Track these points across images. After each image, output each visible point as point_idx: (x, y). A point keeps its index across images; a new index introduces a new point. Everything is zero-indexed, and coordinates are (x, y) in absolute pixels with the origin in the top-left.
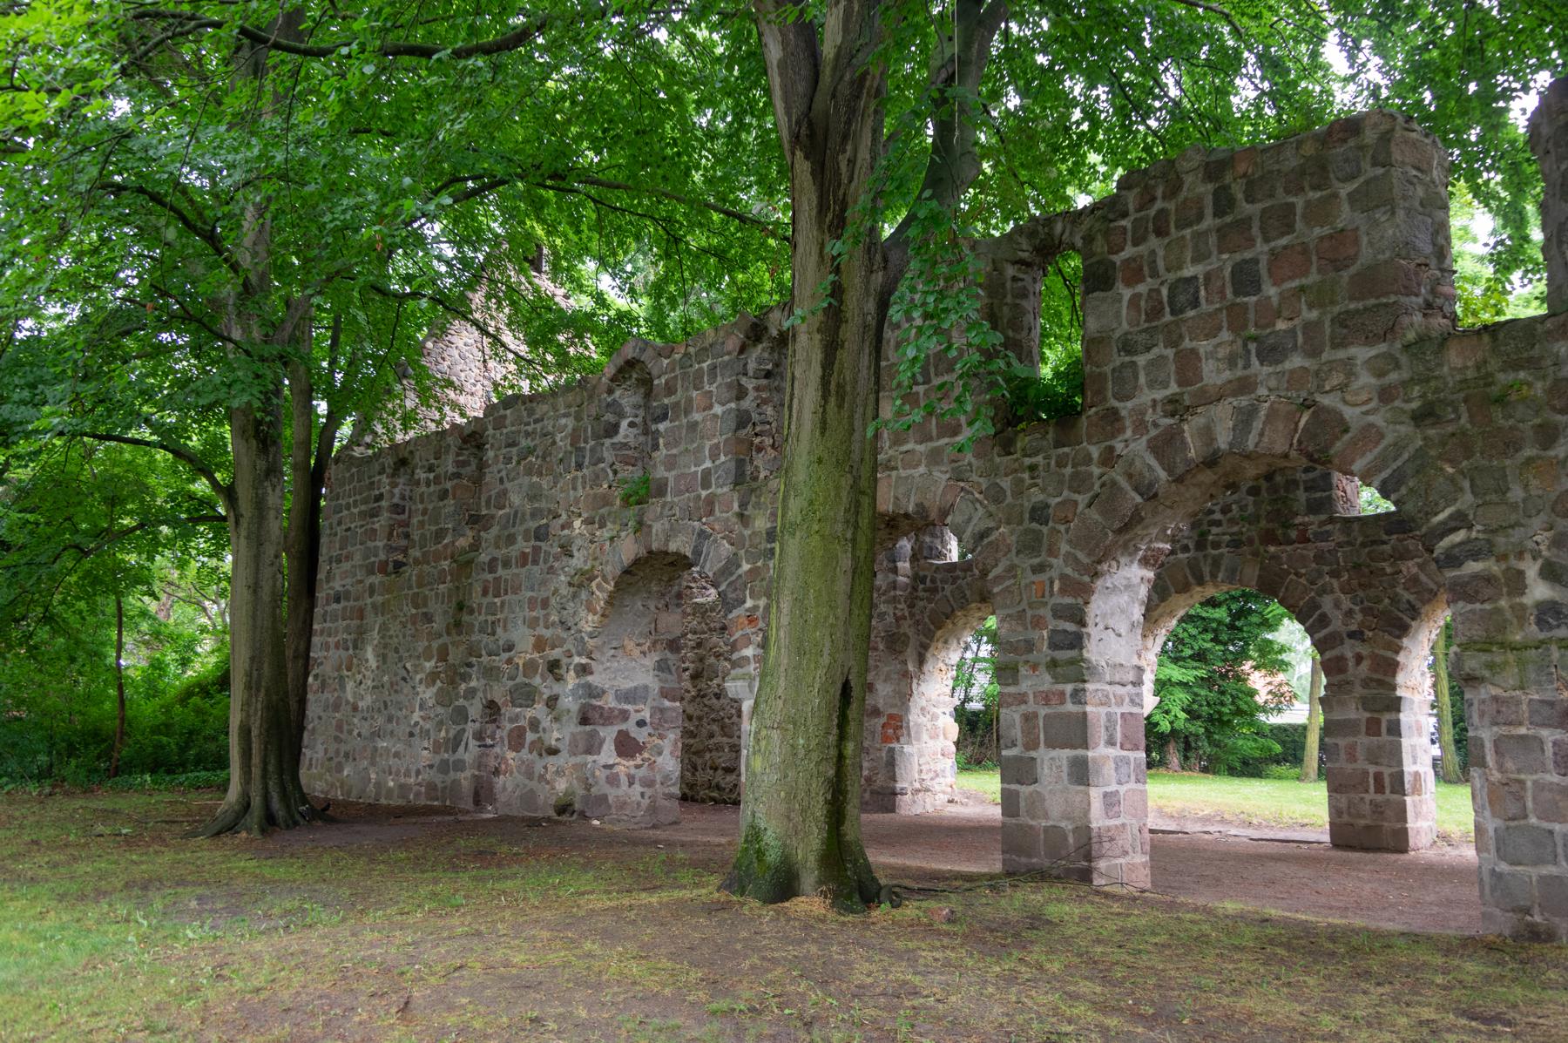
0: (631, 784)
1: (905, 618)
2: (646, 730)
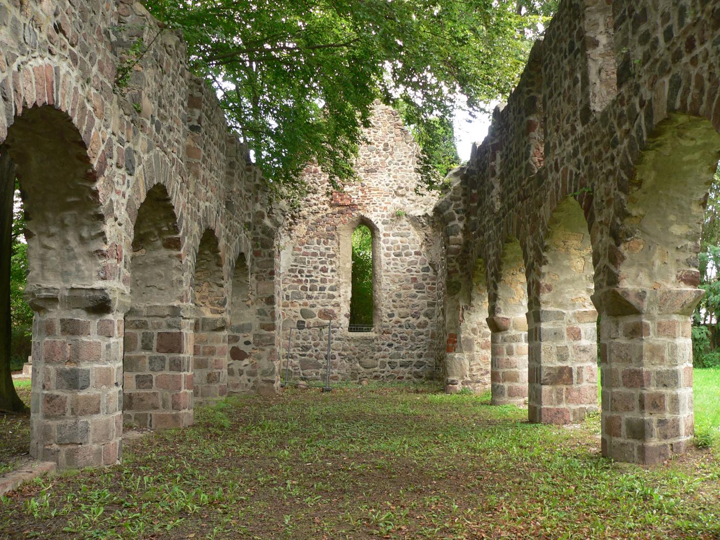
0: (241, 375)
1: (456, 271)
2: (250, 347)
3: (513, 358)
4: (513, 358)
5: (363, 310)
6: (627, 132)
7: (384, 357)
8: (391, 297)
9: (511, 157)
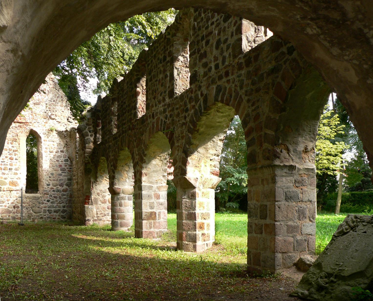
3: (122, 208)
4: (122, 208)
5: (33, 182)
6: (194, 106)
7: (45, 207)
8: (48, 175)
9: (124, 107)
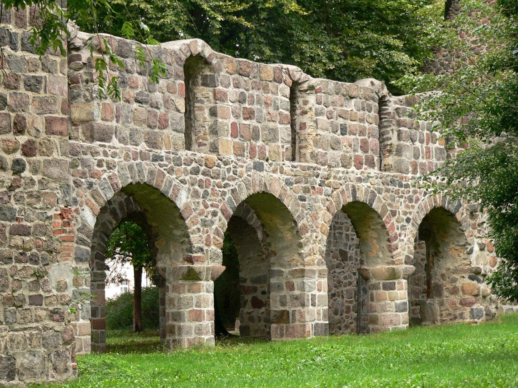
0: (260, 321)
3: (374, 303)
4: (374, 303)
